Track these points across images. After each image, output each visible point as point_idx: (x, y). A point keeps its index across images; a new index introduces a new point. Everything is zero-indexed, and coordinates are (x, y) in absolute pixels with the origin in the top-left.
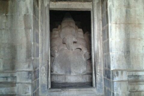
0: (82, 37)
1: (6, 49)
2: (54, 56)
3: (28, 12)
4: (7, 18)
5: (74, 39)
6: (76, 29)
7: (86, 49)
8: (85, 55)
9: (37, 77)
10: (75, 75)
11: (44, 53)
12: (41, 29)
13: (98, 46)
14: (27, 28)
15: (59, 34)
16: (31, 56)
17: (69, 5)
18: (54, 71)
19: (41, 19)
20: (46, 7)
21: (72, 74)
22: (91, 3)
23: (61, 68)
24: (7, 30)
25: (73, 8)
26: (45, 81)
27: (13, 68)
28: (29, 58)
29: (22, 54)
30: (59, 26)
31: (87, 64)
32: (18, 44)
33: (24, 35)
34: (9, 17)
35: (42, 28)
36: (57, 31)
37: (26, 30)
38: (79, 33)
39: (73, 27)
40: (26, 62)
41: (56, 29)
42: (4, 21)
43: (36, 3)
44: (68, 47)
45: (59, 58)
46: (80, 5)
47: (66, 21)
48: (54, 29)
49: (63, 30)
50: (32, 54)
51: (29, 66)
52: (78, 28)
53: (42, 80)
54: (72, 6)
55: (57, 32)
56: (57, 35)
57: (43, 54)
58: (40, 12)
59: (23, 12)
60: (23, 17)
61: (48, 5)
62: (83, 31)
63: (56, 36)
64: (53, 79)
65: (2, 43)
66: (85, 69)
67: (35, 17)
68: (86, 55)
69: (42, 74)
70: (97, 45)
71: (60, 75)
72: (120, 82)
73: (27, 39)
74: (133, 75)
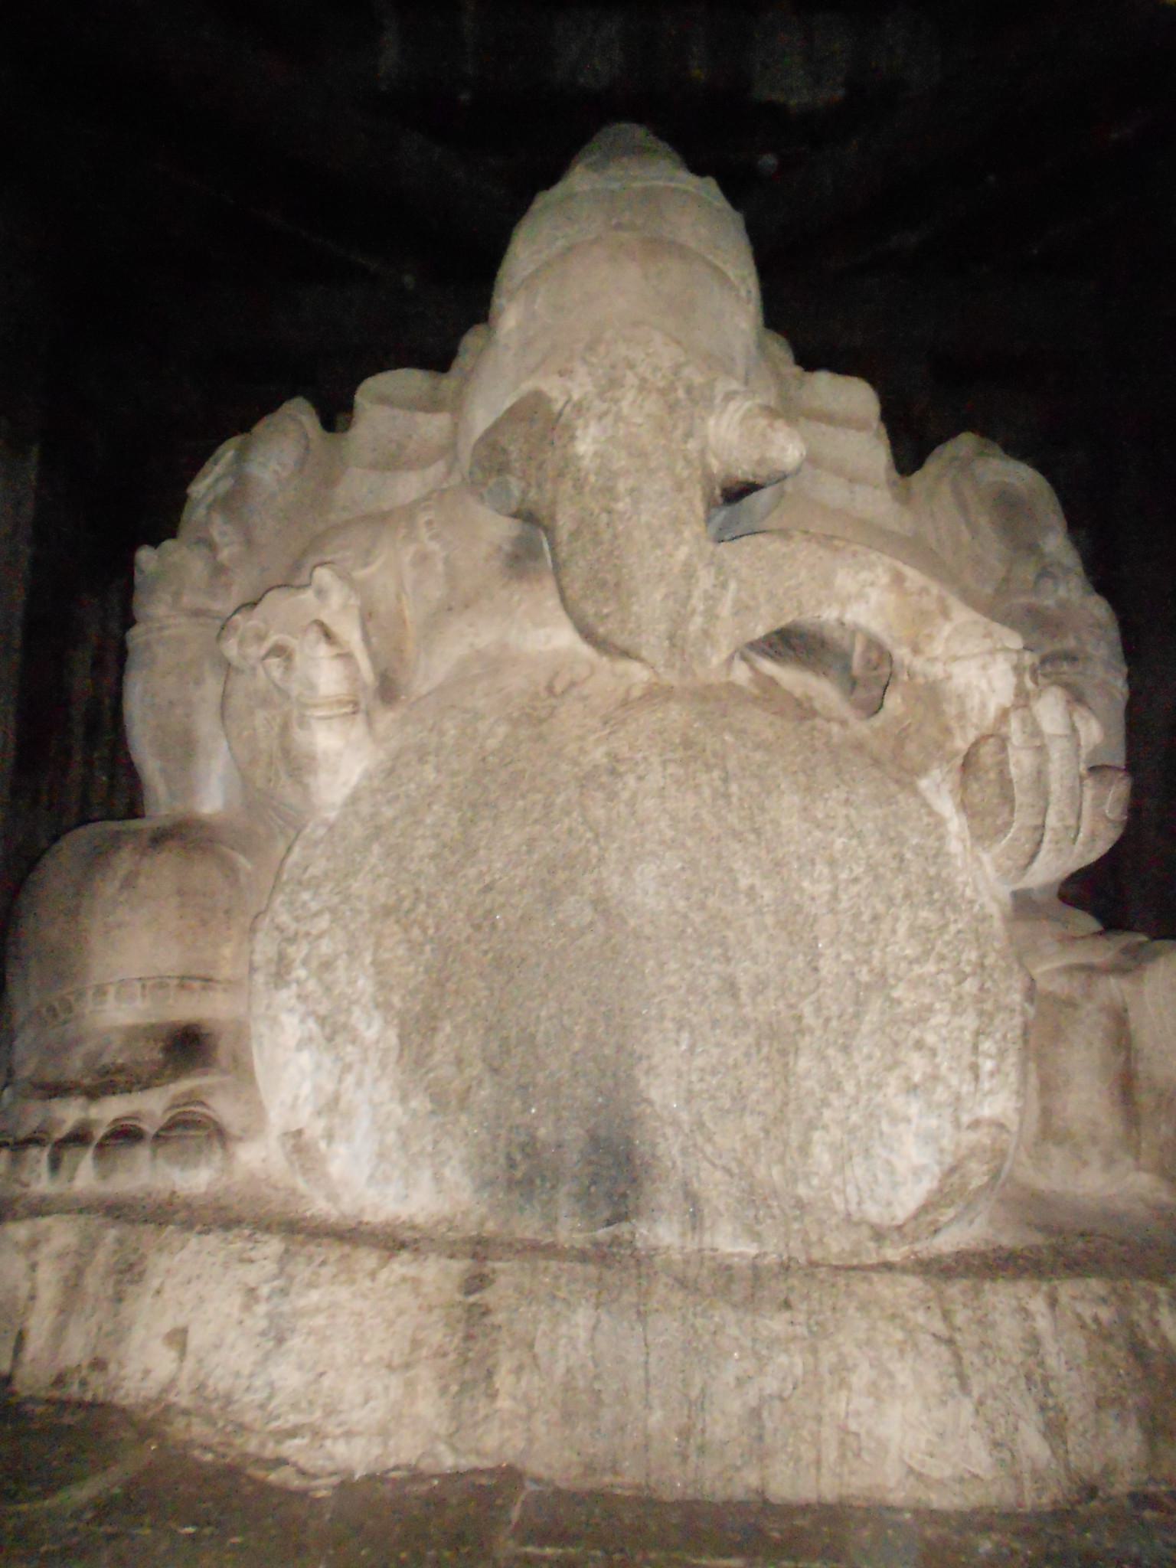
10: (757, 1273)
36: (432, 405)
45: (377, 832)
52: (797, 370)
56: (438, 468)
64: (178, 1338)
68: (1020, 762)
71: (350, 1235)
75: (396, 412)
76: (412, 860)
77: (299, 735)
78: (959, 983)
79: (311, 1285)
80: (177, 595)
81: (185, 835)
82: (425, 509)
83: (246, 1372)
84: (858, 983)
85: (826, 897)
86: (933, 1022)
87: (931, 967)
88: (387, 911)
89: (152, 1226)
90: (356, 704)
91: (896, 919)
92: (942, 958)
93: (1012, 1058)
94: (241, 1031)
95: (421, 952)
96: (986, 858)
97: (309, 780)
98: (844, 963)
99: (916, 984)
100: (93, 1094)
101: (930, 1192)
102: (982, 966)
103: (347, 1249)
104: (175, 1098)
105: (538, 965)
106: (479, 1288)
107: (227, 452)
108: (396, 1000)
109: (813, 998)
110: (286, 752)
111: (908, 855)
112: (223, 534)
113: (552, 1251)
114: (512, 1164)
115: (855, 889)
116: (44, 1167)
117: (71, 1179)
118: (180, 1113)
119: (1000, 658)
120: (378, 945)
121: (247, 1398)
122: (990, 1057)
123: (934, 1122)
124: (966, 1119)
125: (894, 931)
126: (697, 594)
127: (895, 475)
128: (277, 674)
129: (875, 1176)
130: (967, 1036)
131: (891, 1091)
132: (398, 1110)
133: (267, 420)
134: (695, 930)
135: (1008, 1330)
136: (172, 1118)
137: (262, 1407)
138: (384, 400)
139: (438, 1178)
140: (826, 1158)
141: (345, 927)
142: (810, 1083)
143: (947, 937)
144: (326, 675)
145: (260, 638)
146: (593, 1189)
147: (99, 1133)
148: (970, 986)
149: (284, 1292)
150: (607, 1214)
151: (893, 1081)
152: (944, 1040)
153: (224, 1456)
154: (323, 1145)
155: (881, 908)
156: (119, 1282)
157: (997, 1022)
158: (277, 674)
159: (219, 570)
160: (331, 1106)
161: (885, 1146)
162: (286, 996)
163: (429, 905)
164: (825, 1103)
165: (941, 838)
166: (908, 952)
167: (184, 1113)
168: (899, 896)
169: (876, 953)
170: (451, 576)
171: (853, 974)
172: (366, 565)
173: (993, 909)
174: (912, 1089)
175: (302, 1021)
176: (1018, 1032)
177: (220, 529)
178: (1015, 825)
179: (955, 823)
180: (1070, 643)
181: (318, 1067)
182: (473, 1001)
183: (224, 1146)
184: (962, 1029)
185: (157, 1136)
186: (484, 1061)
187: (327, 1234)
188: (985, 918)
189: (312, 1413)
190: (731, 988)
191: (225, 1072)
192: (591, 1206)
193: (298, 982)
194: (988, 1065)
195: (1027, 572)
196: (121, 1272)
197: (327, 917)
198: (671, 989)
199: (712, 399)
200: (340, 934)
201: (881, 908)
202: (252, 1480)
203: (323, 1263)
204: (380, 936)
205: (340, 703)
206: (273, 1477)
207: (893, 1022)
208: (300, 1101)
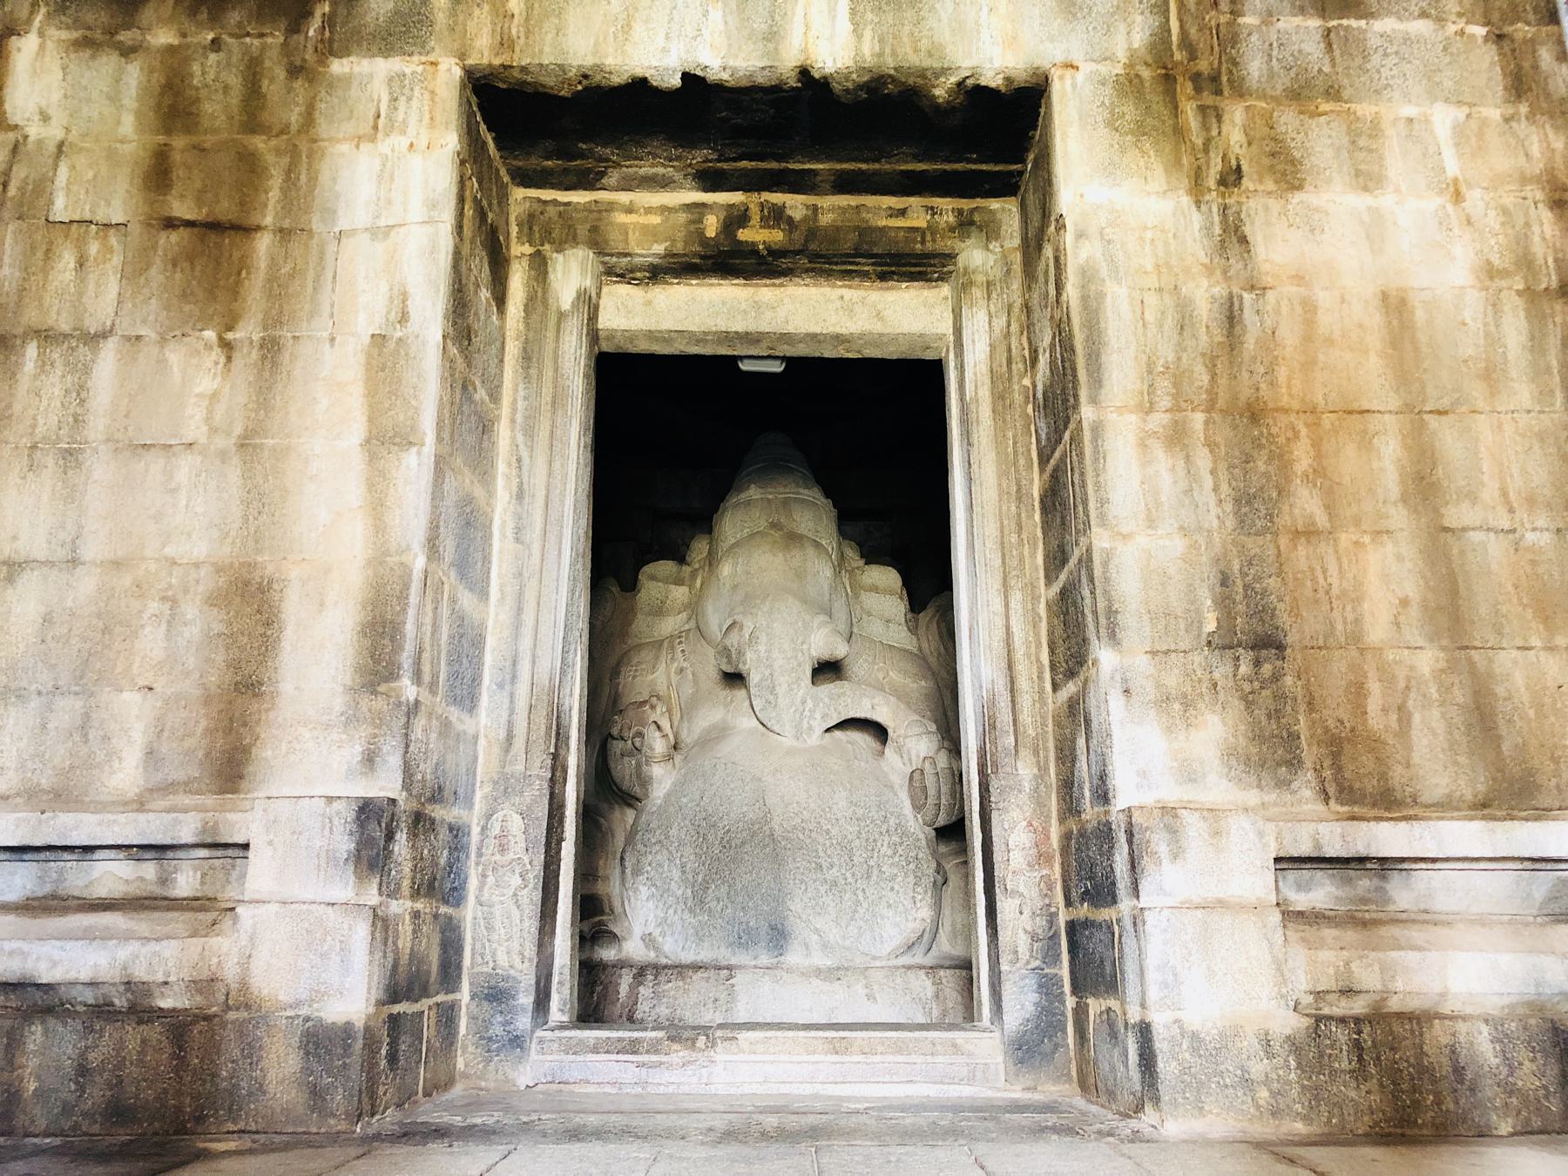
0: (899, 635)
1: (191, 610)
2: (637, 790)
3: (404, 318)
4: (229, 359)
5: (823, 642)
6: (840, 565)
7: (933, 727)
9: (440, 885)
10: (830, 970)
11: (522, 689)
12: (515, 482)
13: (1008, 628)
14: (385, 439)
15: (694, 608)
16: (392, 674)
17: (757, 306)
19: (521, 405)
20: (562, 316)
21: (794, 957)
22: (945, 290)
23: (698, 901)
24: (223, 456)
25: (791, 329)
26: (516, 945)
27: (230, 768)
28: (374, 693)
29: (316, 657)
30: (699, 548)
31: (939, 869)
32: (294, 573)
33: (353, 491)
34: (247, 358)
35: (519, 476)
36: (679, 582)
37: (372, 458)
38: (870, 600)
39: (817, 545)
40: (351, 720)
41: (666, 567)
42: (206, 383)
43: (480, 268)
46: (850, 311)
47: (753, 492)
48: (649, 569)
49: (726, 570)
50: (406, 659)
51: (370, 759)
52: (861, 563)
53: (490, 928)
54: (781, 313)
55: (680, 593)
57: (512, 695)
58: (513, 349)
59: (362, 317)
60: (362, 358)
61: (590, 305)
62: (906, 583)
63: (670, 625)
65: (167, 559)
66: (925, 913)
67: (460, 363)
69: (491, 880)
70: (1000, 622)
72: (1199, 913)
73: (379, 526)
74: (1318, 846)
77: (645, 768)
110: (639, 775)
138: (653, 578)
148: (912, 866)
170: (696, 681)
173: (922, 836)
179: (907, 804)
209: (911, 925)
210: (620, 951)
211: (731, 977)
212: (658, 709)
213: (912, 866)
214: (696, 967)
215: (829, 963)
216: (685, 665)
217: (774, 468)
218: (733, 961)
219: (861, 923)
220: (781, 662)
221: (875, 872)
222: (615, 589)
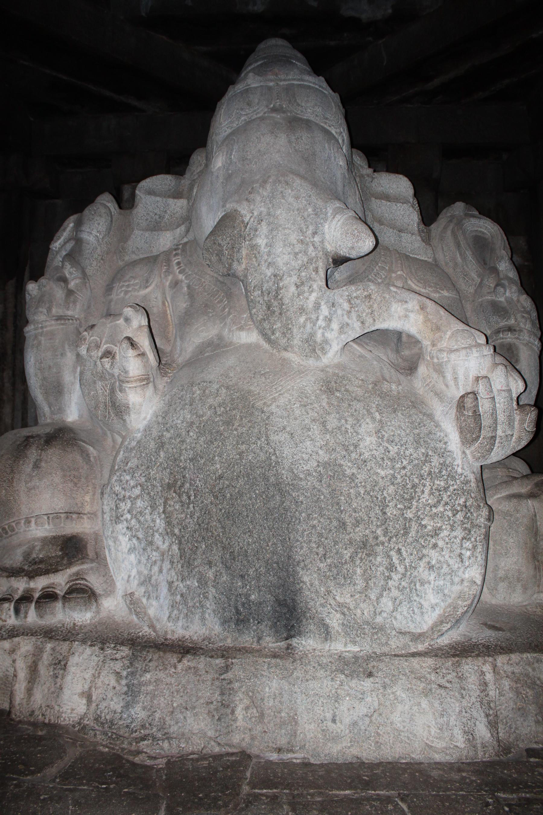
8: (467, 408)
18: (110, 591)
36: (177, 195)
44: (271, 313)
48: (147, 183)
52: (370, 171)
68: (484, 406)
75: (158, 199)
76: (181, 461)
78: (454, 515)
79: (146, 671)
80: (49, 310)
81: (62, 436)
82: (176, 255)
83: (119, 710)
84: (405, 519)
85: (390, 477)
86: (442, 535)
87: (441, 509)
88: (169, 486)
89: (68, 642)
90: (148, 379)
91: (424, 486)
92: (447, 504)
93: (479, 549)
94: (97, 538)
95: (188, 508)
96: (468, 452)
97: (126, 417)
98: (399, 509)
99: (433, 517)
100: (32, 575)
101: (440, 615)
102: (466, 507)
103: (161, 653)
104: (70, 576)
105: (247, 516)
106: (226, 671)
107: (70, 224)
108: (176, 531)
109: (384, 527)
110: (114, 404)
111: (430, 453)
112: (71, 273)
113: (259, 652)
114: (238, 612)
115: (403, 472)
116: (12, 612)
117: (26, 617)
118: (73, 585)
119: (474, 350)
120: (165, 503)
121: (121, 723)
122: (470, 550)
123: (441, 583)
124: (456, 580)
125: (423, 492)
126: (321, 318)
127: (422, 226)
128: (107, 366)
129: (413, 610)
130: (458, 541)
131: (421, 570)
132: (181, 585)
133: (90, 207)
134: (325, 497)
135: (472, 681)
136: (71, 587)
137: (127, 726)
138: (151, 192)
139: (203, 619)
140: (390, 604)
141: (149, 494)
142: (381, 569)
143: (449, 493)
144: (134, 366)
145: (98, 347)
146: (278, 623)
147: (37, 595)
148: (460, 516)
149: (133, 674)
150: (285, 635)
151: (422, 564)
152: (447, 543)
153: (113, 749)
154: (144, 600)
155: (416, 481)
156: (55, 669)
157: (472, 533)
158: (107, 366)
159: (70, 293)
160: (146, 581)
161: (418, 595)
162: (121, 527)
163: (191, 484)
164: (389, 578)
165: (446, 443)
166: (430, 501)
167: (77, 584)
168: (426, 474)
169: (414, 503)
170: (191, 295)
171: (403, 514)
172: (147, 287)
173: (472, 477)
174: (431, 567)
175: (130, 540)
176: (482, 537)
177: (69, 271)
178: (482, 437)
180: (512, 322)
181: (139, 562)
182: (216, 533)
183: (96, 601)
184: (455, 537)
185: (64, 597)
186: (222, 563)
187: (151, 647)
188: (468, 482)
189: (152, 729)
190: (343, 525)
191: (92, 561)
192: (277, 632)
193: (126, 520)
194: (468, 553)
195: (491, 282)
196: (55, 664)
197: (139, 488)
198: (314, 527)
199: (326, 214)
200: (146, 497)
201: (416, 481)
202: (128, 761)
203: (150, 661)
204: (166, 499)
205: (142, 380)
206: (137, 760)
207: (422, 537)
208: (132, 577)
209: (457, 588)
210: (98, 612)
211: (227, 668)
212: (135, 323)
213: (460, 516)
214: (185, 649)
215: (356, 649)
216: (181, 277)
217: (276, 45)
218: (229, 642)
219: (395, 593)
220: (286, 257)
221: (414, 527)
222: (112, 205)
